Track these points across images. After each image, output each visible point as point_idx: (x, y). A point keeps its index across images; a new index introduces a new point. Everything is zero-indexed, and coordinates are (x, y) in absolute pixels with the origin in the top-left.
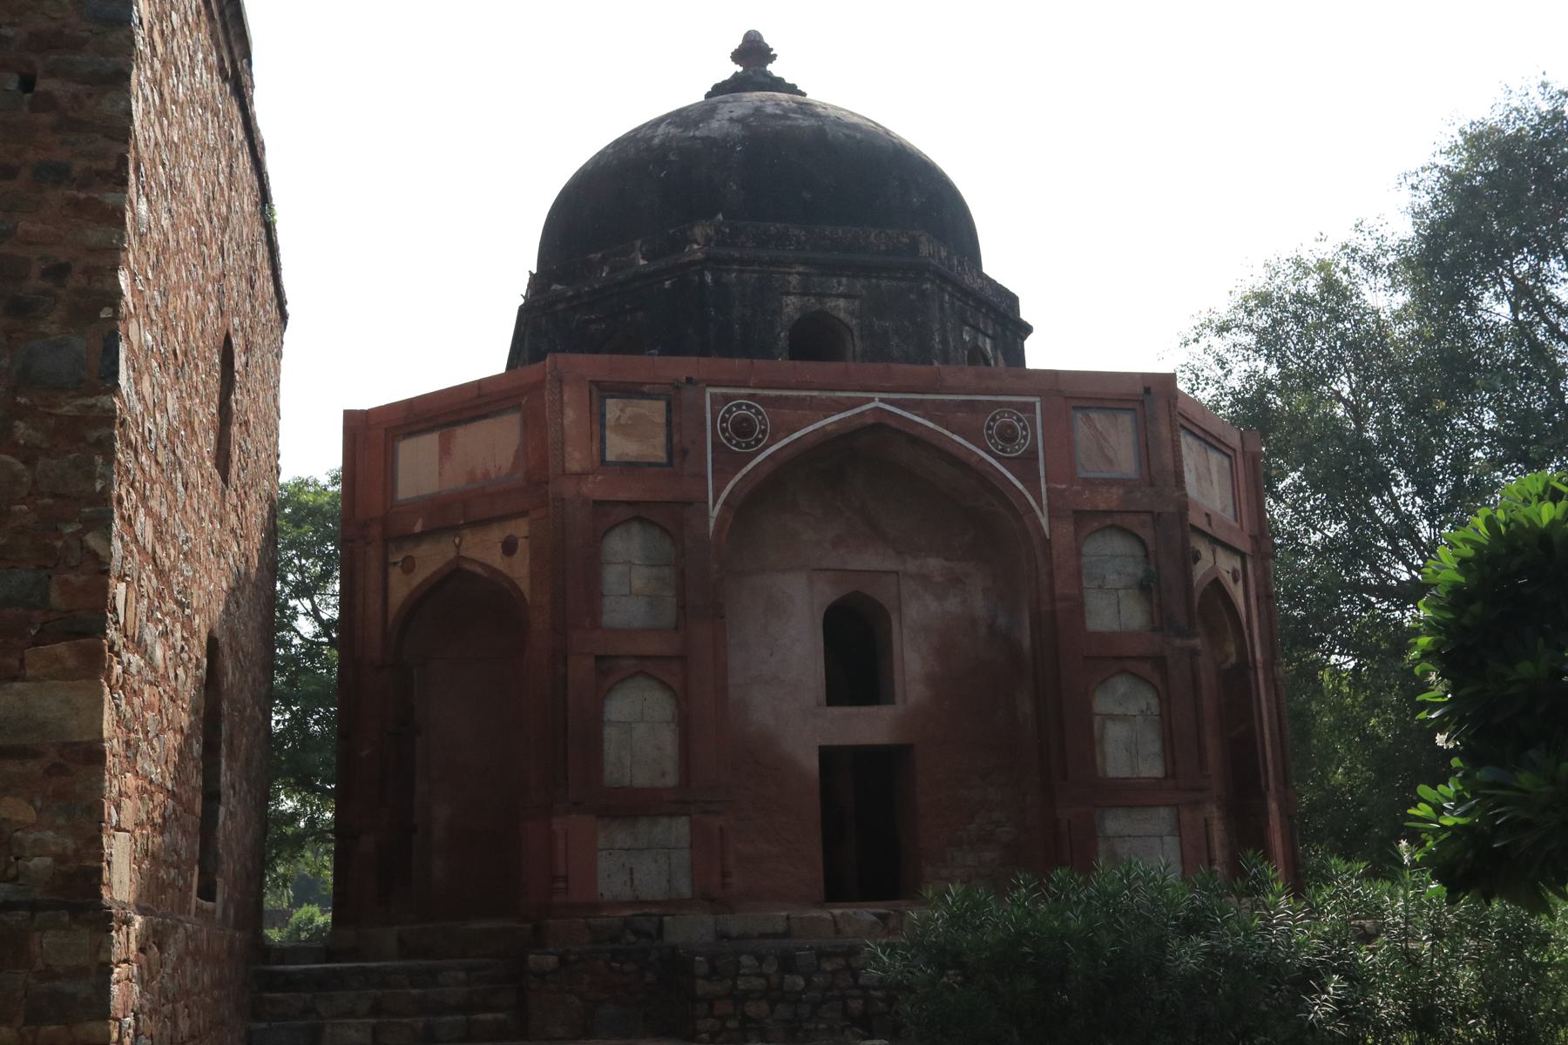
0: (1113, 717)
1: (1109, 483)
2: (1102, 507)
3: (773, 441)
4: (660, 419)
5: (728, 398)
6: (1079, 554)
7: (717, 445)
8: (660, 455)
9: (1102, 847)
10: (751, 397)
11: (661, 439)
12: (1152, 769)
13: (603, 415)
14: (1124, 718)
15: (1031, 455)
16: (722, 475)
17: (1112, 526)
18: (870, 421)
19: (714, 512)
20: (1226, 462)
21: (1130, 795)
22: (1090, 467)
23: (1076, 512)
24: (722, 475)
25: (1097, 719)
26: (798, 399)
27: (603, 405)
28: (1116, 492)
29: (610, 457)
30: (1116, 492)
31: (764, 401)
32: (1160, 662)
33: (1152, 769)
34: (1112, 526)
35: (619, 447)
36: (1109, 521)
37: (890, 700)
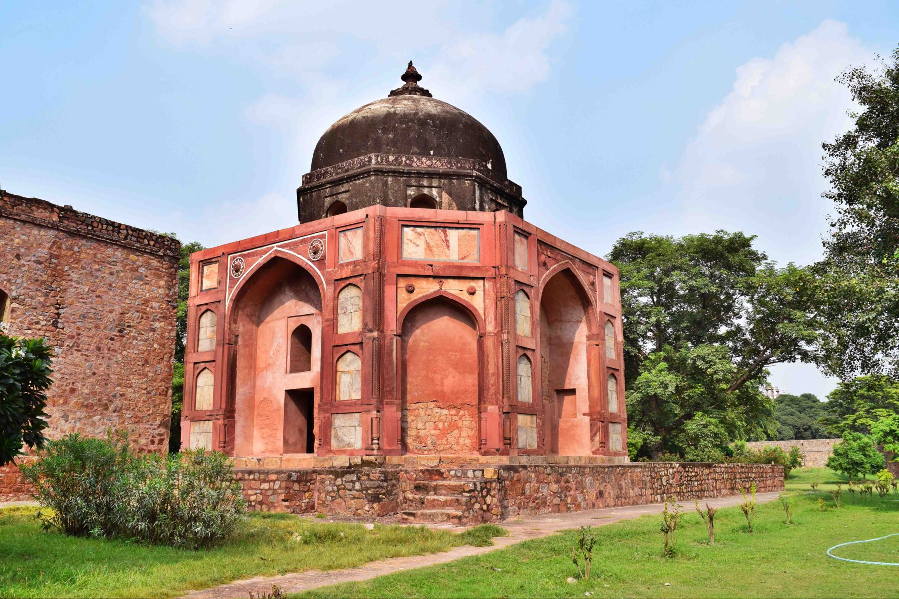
0: (343, 372)
1: (348, 264)
2: (344, 276)
4: (217, 270)
5: (234, 257)
6: (336, 298)
7: (231, 276)
8: (215, 284)
9: (333, 432)
12: (357, 396)
14: (349, 372)
15: (323, 259)
16: (231, 287)
17: (350, 284)
19: (228, 303)
20: (475, 232)
21: (348, 408)
22: (344, 258)
24: (231, 287)
25: (338, 374)
27: (203, 269)
28: (351, 267)
30: (351, 267)
31: (244, 256)
32: (361, 344)
33: (357, 396)
34: (350, 284)
35: (207, 284)
36: (348, 282)
37: (309, 369)
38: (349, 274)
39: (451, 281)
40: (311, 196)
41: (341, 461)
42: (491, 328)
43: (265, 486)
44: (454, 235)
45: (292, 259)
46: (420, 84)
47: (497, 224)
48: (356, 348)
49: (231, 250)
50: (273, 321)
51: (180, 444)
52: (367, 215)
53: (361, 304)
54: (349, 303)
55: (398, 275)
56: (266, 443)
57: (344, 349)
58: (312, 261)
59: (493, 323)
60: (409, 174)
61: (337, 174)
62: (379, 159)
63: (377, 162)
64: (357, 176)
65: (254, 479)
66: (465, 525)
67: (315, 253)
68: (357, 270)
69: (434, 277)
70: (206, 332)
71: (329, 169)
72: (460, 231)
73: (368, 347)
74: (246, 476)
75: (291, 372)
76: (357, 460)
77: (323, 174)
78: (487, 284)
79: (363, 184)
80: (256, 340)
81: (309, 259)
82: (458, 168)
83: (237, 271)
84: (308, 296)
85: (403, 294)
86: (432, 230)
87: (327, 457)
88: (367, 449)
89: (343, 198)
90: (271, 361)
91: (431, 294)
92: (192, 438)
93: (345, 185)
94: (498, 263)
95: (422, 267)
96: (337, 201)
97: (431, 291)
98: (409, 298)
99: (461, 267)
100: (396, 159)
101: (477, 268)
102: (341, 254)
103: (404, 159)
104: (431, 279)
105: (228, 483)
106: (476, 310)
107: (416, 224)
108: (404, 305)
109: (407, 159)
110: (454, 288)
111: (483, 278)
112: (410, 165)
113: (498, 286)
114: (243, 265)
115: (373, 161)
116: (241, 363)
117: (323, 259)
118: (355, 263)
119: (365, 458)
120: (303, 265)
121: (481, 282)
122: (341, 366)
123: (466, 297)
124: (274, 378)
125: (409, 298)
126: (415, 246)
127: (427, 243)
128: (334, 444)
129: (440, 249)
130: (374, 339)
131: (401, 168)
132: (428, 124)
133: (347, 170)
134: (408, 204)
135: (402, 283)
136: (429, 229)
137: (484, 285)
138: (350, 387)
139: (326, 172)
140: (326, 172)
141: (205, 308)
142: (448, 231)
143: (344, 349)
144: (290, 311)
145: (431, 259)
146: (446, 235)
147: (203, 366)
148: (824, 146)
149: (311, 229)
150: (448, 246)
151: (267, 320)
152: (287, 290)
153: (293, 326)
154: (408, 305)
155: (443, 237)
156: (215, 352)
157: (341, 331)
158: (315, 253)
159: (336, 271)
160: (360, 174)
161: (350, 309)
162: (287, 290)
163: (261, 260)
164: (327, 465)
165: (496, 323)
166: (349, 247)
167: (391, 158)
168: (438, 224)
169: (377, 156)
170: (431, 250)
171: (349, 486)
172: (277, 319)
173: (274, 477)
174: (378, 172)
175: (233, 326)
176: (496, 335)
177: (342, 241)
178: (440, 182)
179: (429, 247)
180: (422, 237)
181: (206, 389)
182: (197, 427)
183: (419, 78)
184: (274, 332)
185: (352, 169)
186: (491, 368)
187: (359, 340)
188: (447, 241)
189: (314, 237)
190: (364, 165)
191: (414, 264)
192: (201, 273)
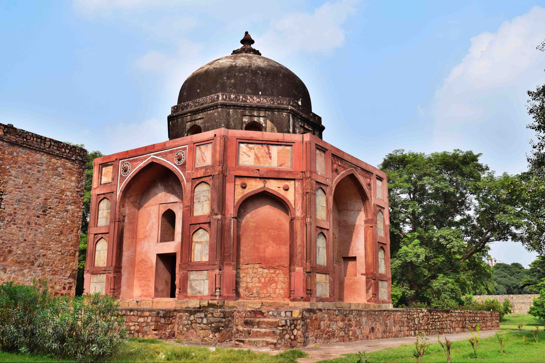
0: (197, 242)
1: (202, 168)
2: (199, 176)
3: (131, 172)
4: (111, 171)
5: (124, 162)
6: (193, 191)
9: (189, 283)
10: (127, 161)
11: (111, 177)
12: (206, 259)
13: (102, 172)
14: (201, 243)
15: (184, 164)
16: (121, 183)
18: (150, 161)
21: (199, 267)
22: (199, 164)
23: (193, 179)
24: (121, 183)
25: (193, 243)
26: (137, 159)
27: (102, 170)
28: (203, 170)
29: (102, 183)
30: (203, 170)
32: (209, 223)
33: (206, 259)
35: (104, 180)
36: (201, 180)
37: (173, 240)
38: (202, 175)
39: (272, 181)
40: (177, 121)
41: (194, 304)
42: (299, 213)
43: (141, 320)
44: (274, 150)
45: (163, 164)
46: (253, 46)
47: (304, 143)
48: (206, 226)
49: (120, 157)
50: (149, 206)
51: (84, 290)
52: (215, 135)
53: (210, 196)
54: (202, 195)
55: (236, 176)
56: (143, 291)
57: (198, 226)
58: (177, 166)
59: (300, 211)
60: (244, 107)
61: (195, 106)
62: (224, 97)
63: (223, 99)
64: (209, 108)
65: (133, 315)
66: (278, 349)
67: (179, 160)
68: (207, 173)
69: (260, 178)
70: (103, 213)
71: (190, 103)
72: (279, 147)
73: (214, 225)
74: (128, 313)
75: (161, 242)
76: (205, 303)
77: (186, 107)
78: (296, 184)
79: (213, 114)
80: (137, 219)
81: (175, 165)
82: (278, 104)
83: (125, 171)
84: (174, 189)
85: (239, 190)
86: (260, 146)
87: (185, 300)
88: (212, 296)
89: (199, 123)
90: (147, 235)
91: (258, 190)
92: (92, 286)
93: (201, 114)
94: (304, 170)
95: (252, 171)
96: (195, 125)
97: (258, 187)
98: (243, 192)
99: (279, 172)
100: (236, 97)
101: (290, 172)
102: (197, 161)
103: (241, 97)
104: (258, 179)
105: (116, 318)
106: (289, 201)
107: (248, 141)
108: (240, 197)
109: (243, 97)
110: (274, 186)
111: (294, 180)
112: (246, 101)
113: (304, 185)
114: (129, 167)
115: (220, 98)
116: (126, 235)
117: (184, 164)
118: (206, 168)
119: (210, 302)
120: (171, 168)
121: (293, 182)
122: (196, 238)
123: (282, 192)
124: (149, 245)
125: (243, 192)
126: (248, 157)
127: (256, 155)
128: (189, 291)
129: (265, 159)
130: (218, 220)
131: (239, 103)
132: (258, 73)
133: (202, 104)
134: (244, 128)
135: (239, 182)
136: (257, 145)
137: (295, 184)
138: (201, 252)
139: (188, 105)
140: (188, 105)
141: (102, 197)
142: (271, 147)
143: (198, 226)
144: (161, 199)
145: (258, 165)
146: (269, 149)
147: (100, 236)
148: (529, 93)
149: (177, 144)
150: (270, 157)
151: (146, 205)
152: (159, 185)
153: (163, 209)
154: (241, 198)
155: (267, 151)
156: (109, 227)
157: (196, 214)
158: (179, 160)
159: (193, 173)
160: (211, 107)
161: (202, 198)
162: (159, 185)
163: (142, 164)
164: (184, 306)
165: (303, 210)
166: (203, 158)
167: (232, 96)
168: (264, 142)
169: (223, 95)
170: (258, 160)
171: (199, 321)
172: (152, 205)
173: (147, 314)
174: (223, 105)
175: (122, 209)
176: (302, 218)
177: (198, 152)
178: (265, 113)
179: (257, 158)
180: (252, 151)
181: (102, 252)
182: (95, 278)
183: (253, 42)
184: (150, 214)
185: (206, 103)
186: (299, 242)
187: (208, 221)
188: (270, 154)
189: (179, 149)
190: (214, 101)
191: (247, 169)
192: (100, 172)
